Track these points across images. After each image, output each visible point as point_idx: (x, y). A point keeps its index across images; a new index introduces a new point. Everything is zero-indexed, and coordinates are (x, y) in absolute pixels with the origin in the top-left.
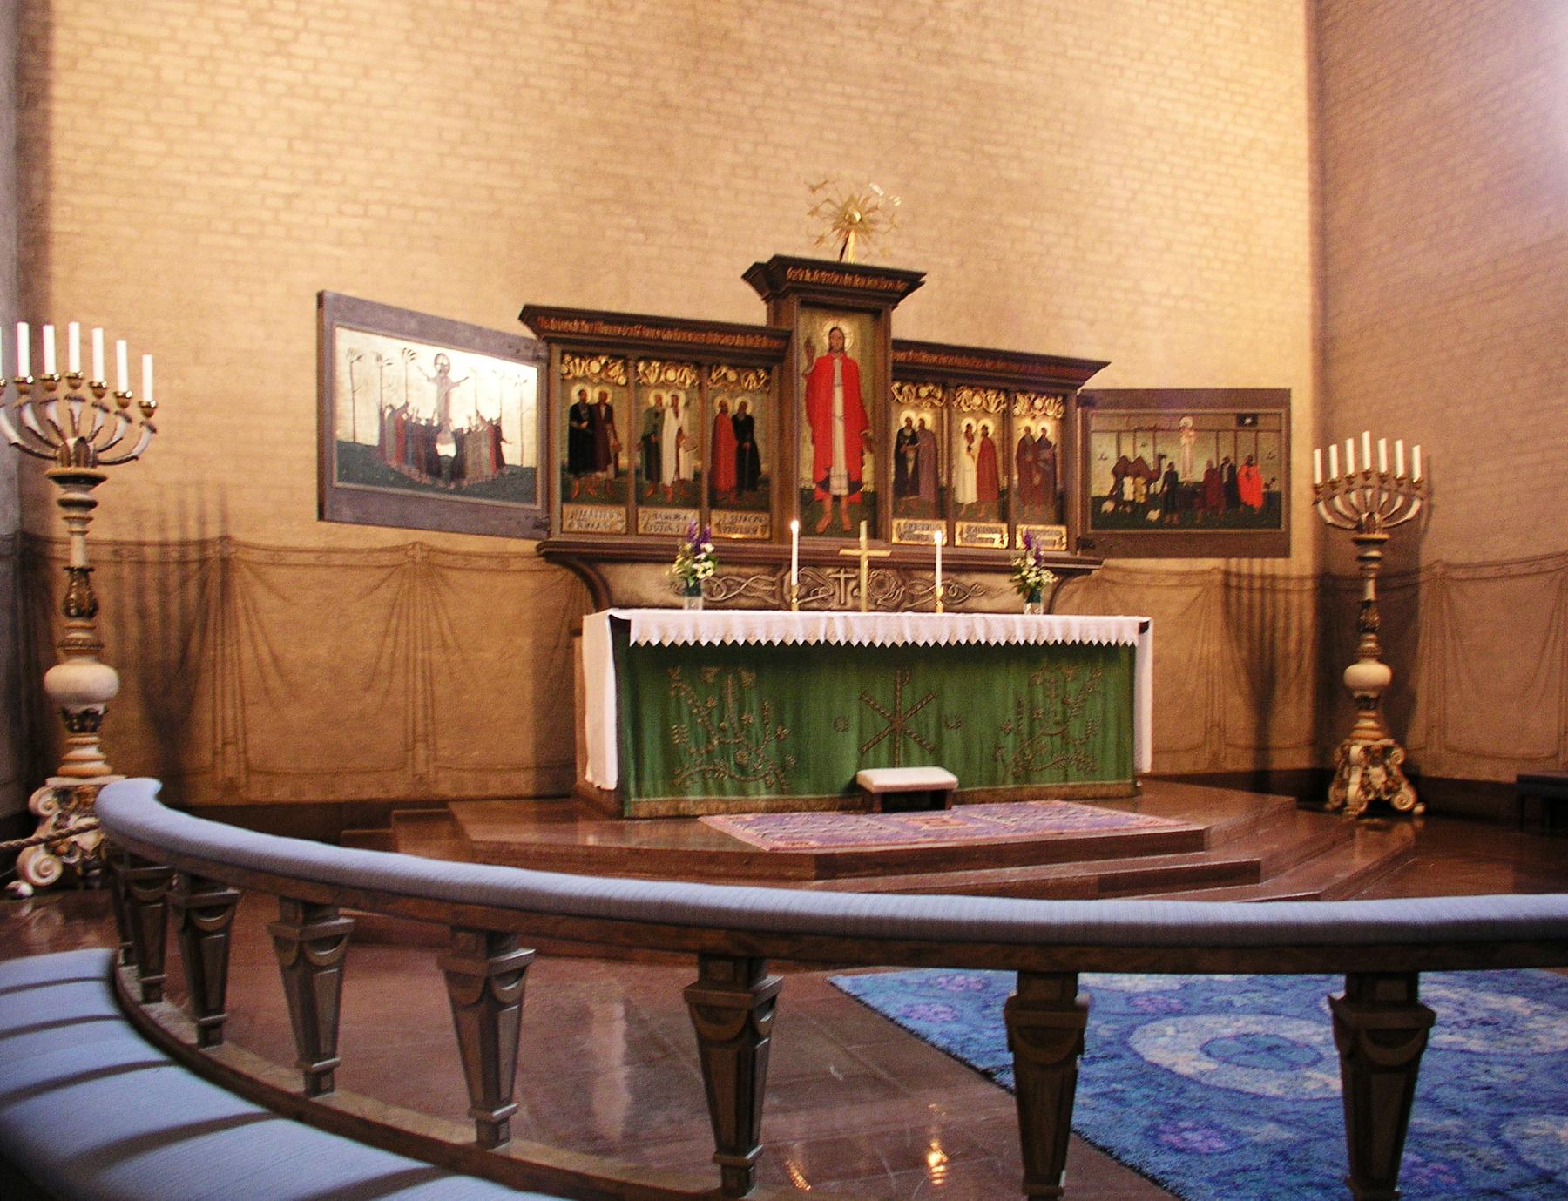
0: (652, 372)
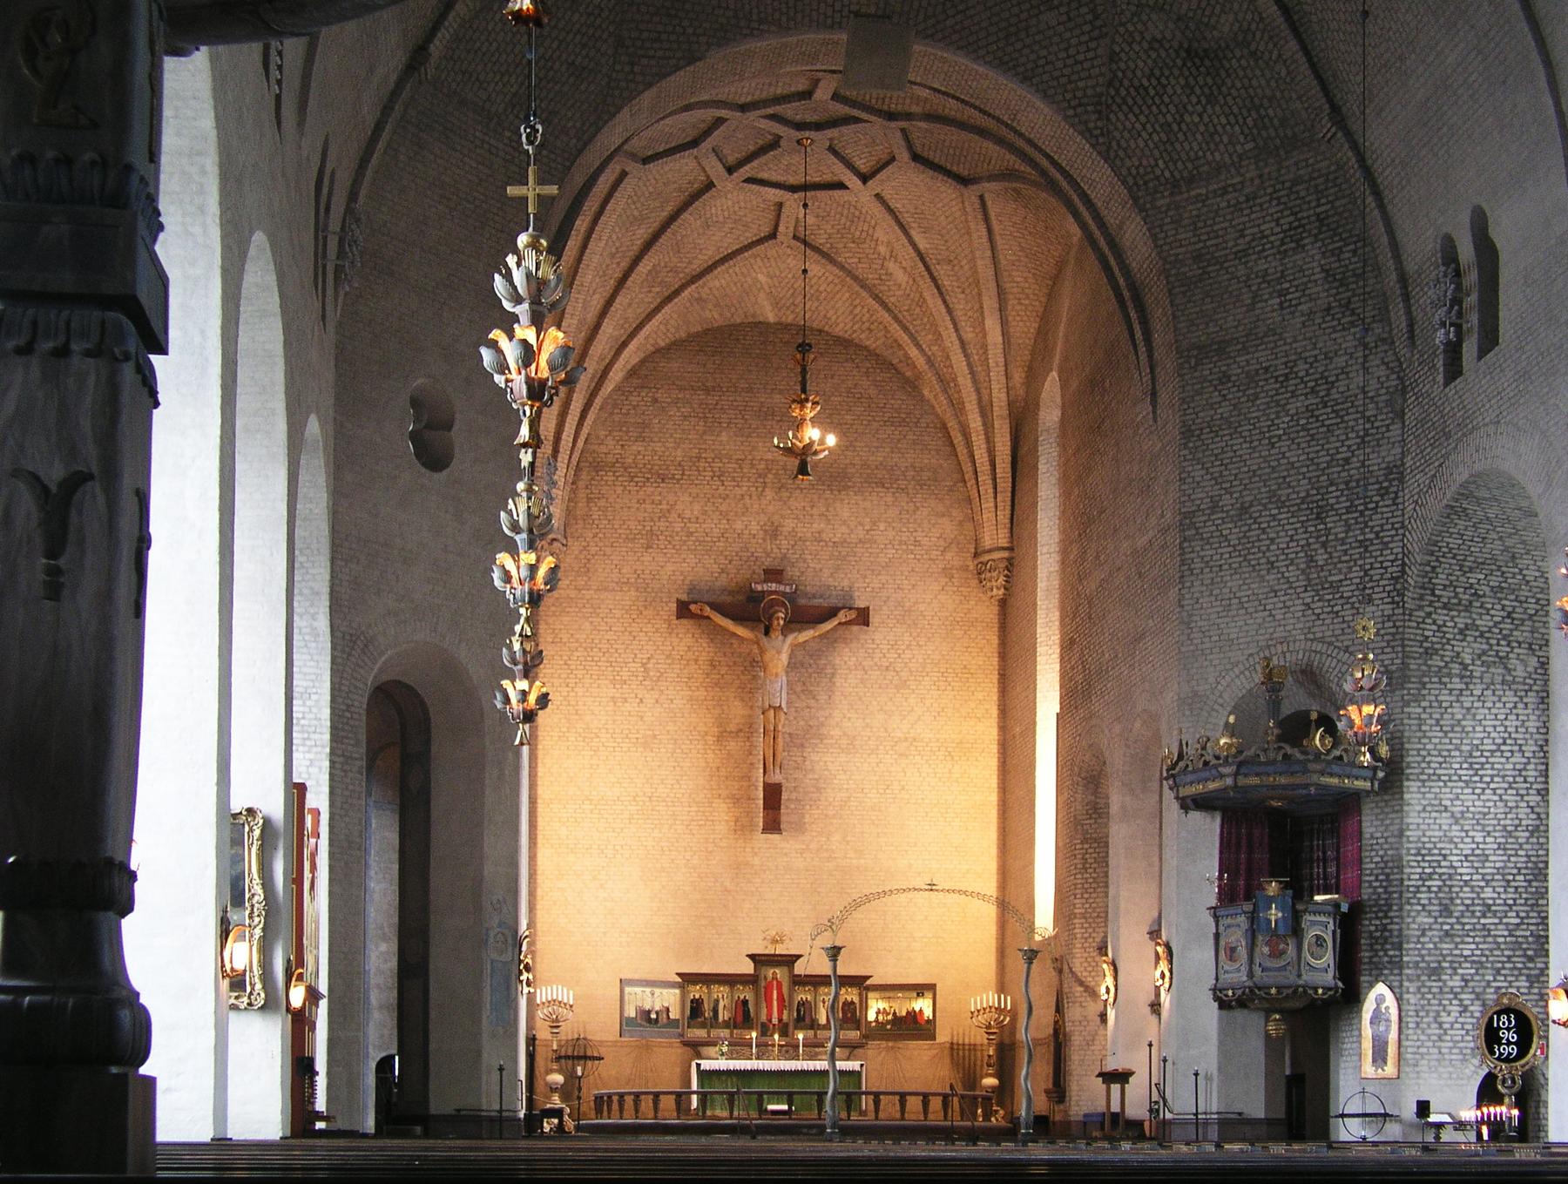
0: (715, 988)
